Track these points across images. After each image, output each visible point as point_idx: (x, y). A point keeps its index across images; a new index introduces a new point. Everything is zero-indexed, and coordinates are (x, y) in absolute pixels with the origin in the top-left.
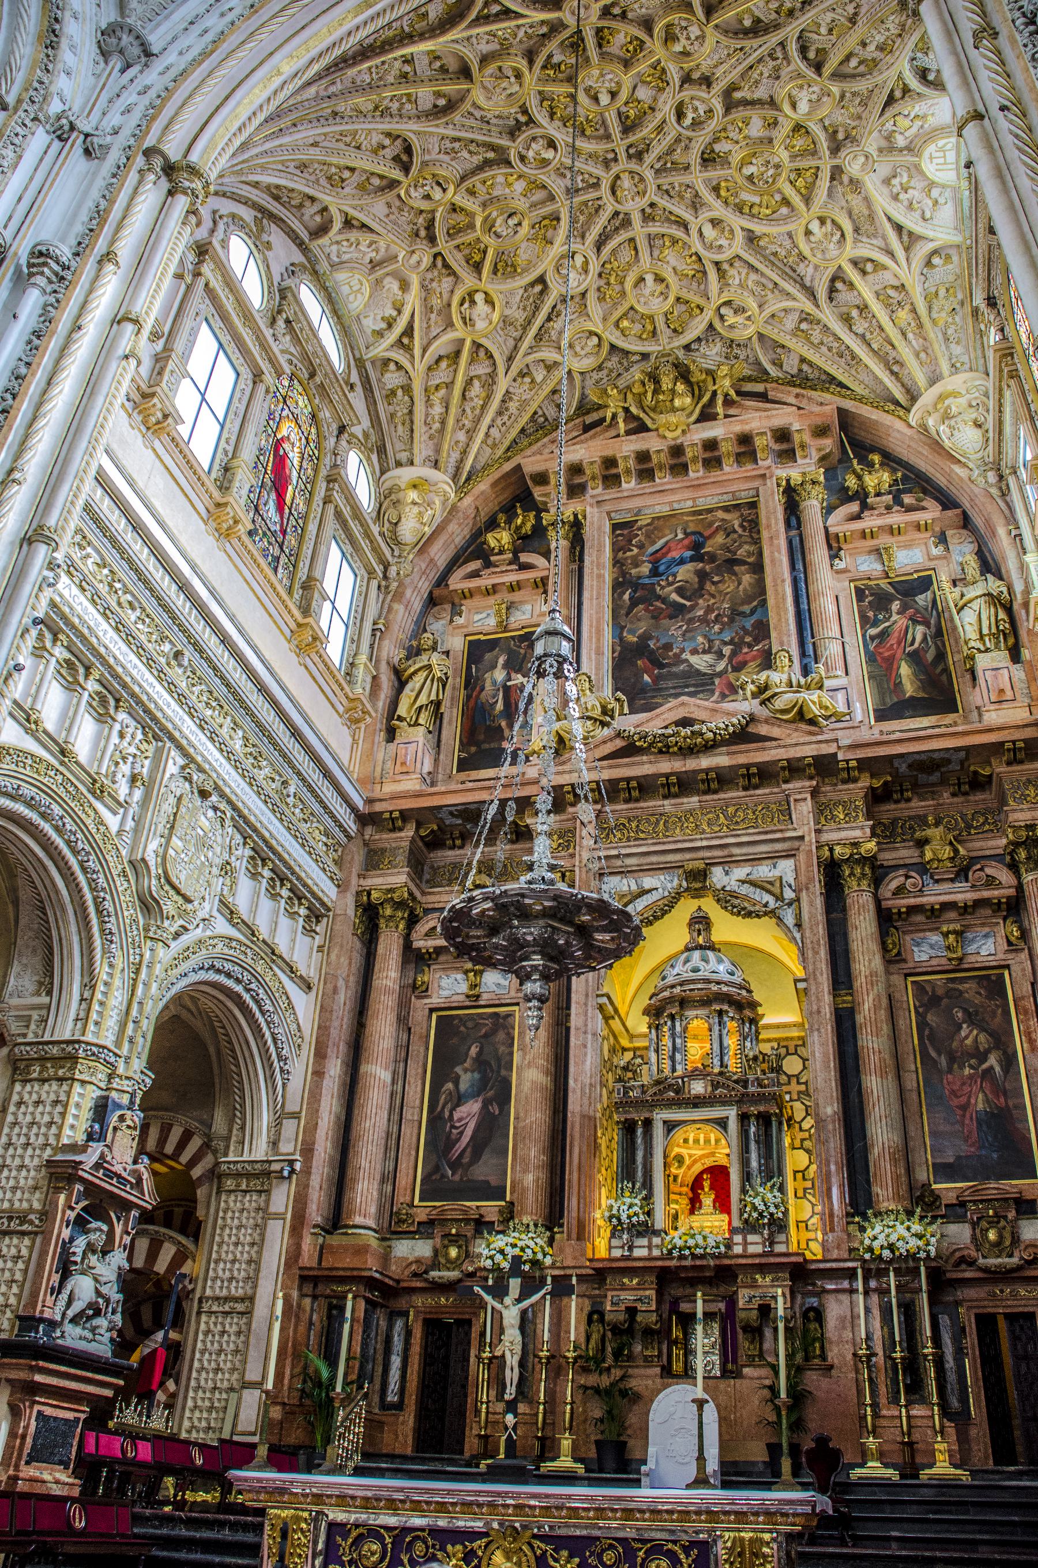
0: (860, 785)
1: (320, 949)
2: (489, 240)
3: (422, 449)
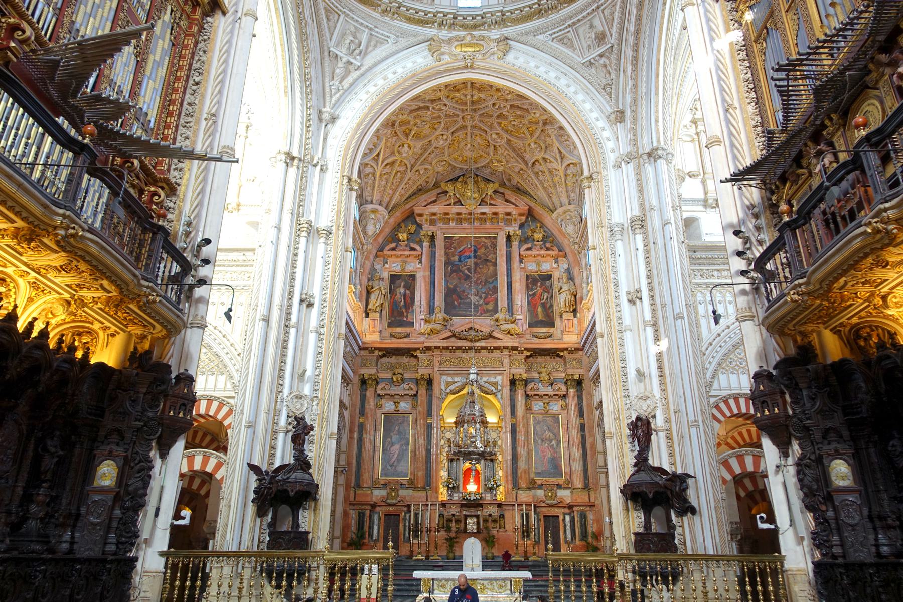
1: (349, 395)
2: (415, 128)
3: (376, 198)
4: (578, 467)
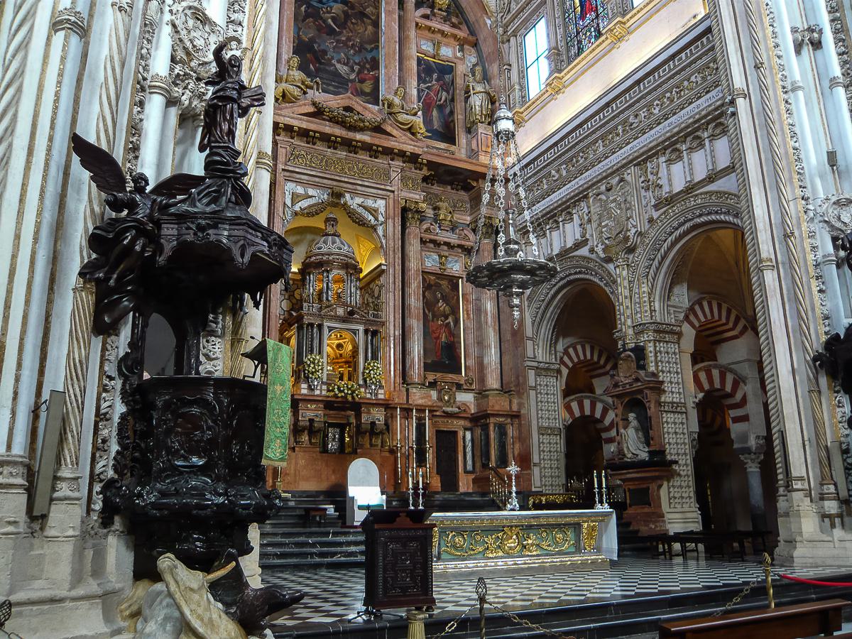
0: (422, 173)
4: (492, 356)
